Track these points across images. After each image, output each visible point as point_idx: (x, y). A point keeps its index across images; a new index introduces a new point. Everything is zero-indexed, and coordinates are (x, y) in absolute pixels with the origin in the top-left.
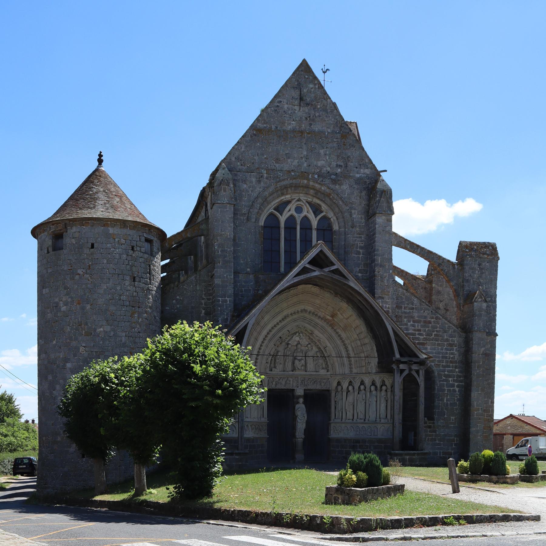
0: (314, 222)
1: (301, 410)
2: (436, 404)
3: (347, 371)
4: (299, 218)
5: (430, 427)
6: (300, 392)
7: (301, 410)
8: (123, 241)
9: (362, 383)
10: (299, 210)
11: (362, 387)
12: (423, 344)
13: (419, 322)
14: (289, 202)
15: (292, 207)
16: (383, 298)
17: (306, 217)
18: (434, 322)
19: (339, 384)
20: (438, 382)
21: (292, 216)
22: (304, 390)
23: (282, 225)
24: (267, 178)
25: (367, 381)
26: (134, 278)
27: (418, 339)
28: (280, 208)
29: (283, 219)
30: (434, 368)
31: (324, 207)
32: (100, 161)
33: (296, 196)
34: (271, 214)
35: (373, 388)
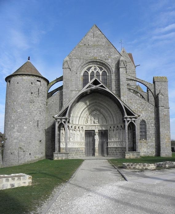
0: (101, 73)
1: (97, 137)
2: (147, 134)
3: (113, 123)
4: (95, 72)
5: (145, 142)
6: (97, 131)
7: (97, 137)
8: (28, 81)
9: (118, 127)
10: (95, 69)
11: (118, 128)
12: (141, 112)
13: (139, 104)
14: (91, 67)
15: (93, 68)
16: (124, 96)
17: (97, 71)
18: (145, 104)
19: (110, 127)
20: (148, 126)
21: (93, 71)
22: (98, 130)
23: (89, 75)
24: (83, 60)
25: (119, 126)
26: (32, 93)
27: (139, 110)
28: (89, 69)
29: (89, 73)
30: (146, 121)
31: (103, 68)
32: (29, 59)
33: (94, 65)
34: (86, 71)
35: (121, 128)
